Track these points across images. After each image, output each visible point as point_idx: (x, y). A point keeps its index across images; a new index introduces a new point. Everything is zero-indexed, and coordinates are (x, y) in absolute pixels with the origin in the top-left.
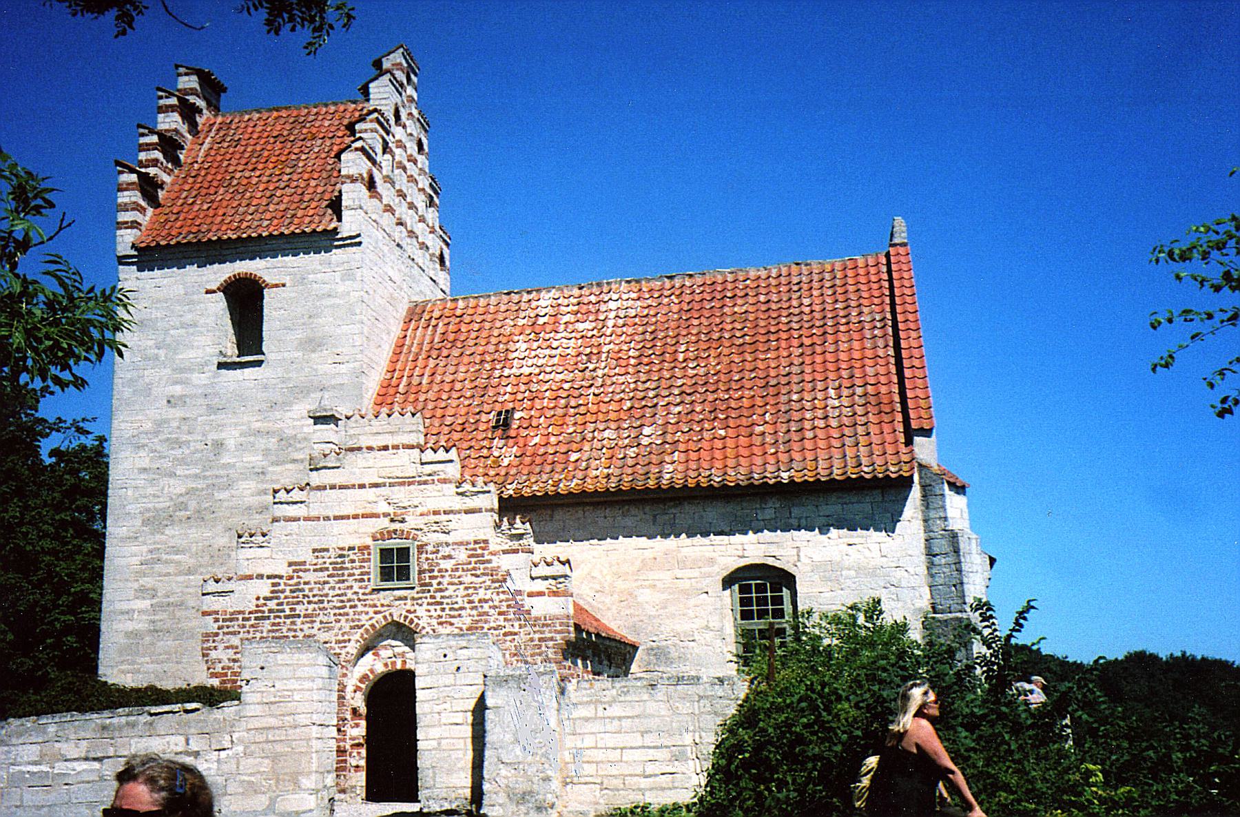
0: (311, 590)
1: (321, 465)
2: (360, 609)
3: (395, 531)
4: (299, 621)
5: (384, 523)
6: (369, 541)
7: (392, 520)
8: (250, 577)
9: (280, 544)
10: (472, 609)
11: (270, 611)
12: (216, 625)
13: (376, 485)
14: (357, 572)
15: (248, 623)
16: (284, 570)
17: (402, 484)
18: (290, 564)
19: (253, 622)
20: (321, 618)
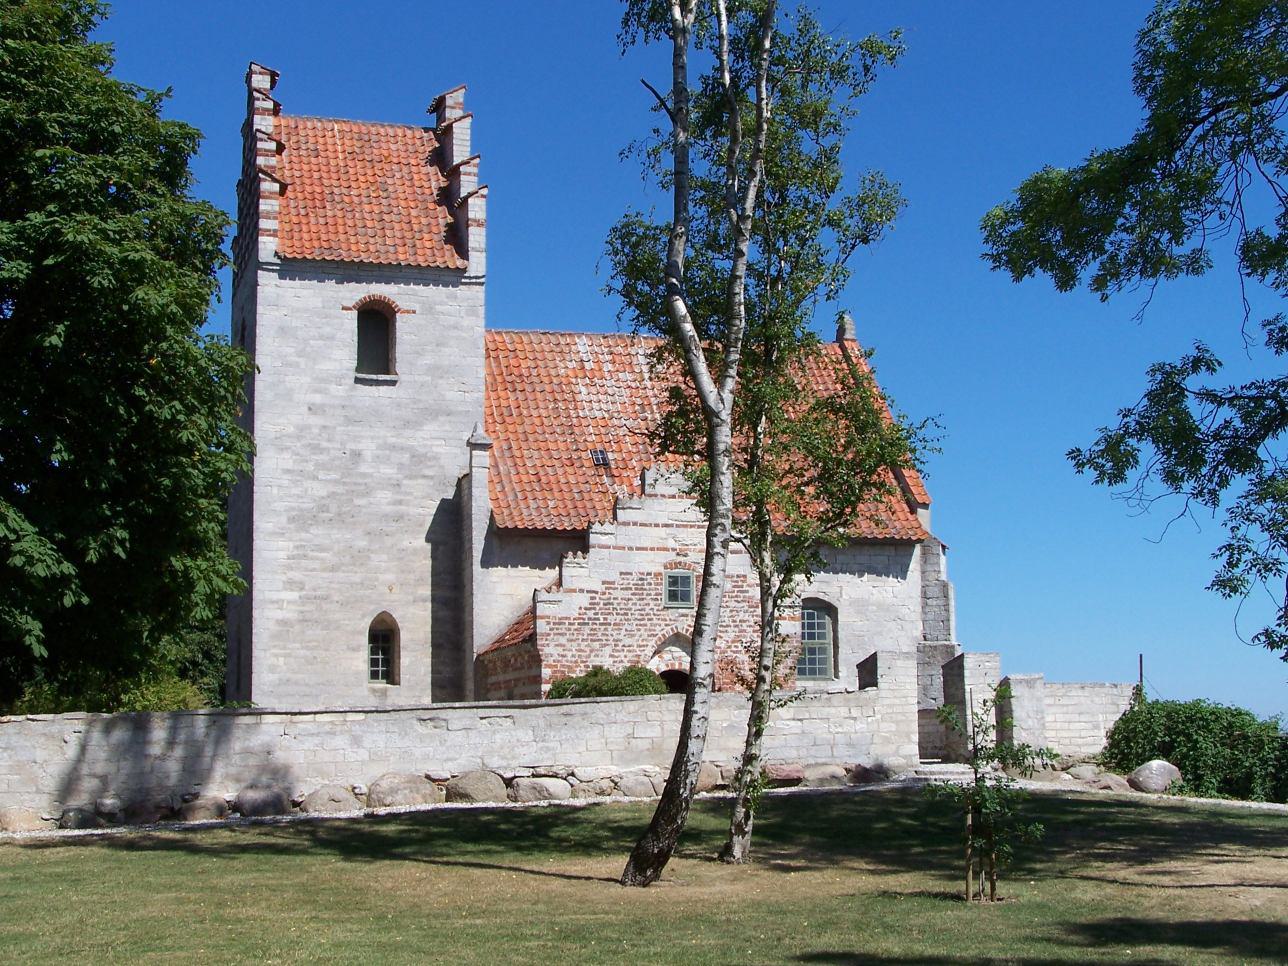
0: (619, 604)
1: (628, 505)
2: (655, 621)
3: (680, 563)
4: (610, 628)
5: (672, 556)
6: (662, 570)
7: (678, 554)
8: (574, 591)
9: (595, 566)
10: (736, 626)
11: (590, 619)
12: (548, 627)
13: (666, 526)
14: (653, 593)
15: (573, 627)
16: (600, 587)
17: (686, 526)
18: (604, 583)
19: (576, 626)
20: (626, 626)
